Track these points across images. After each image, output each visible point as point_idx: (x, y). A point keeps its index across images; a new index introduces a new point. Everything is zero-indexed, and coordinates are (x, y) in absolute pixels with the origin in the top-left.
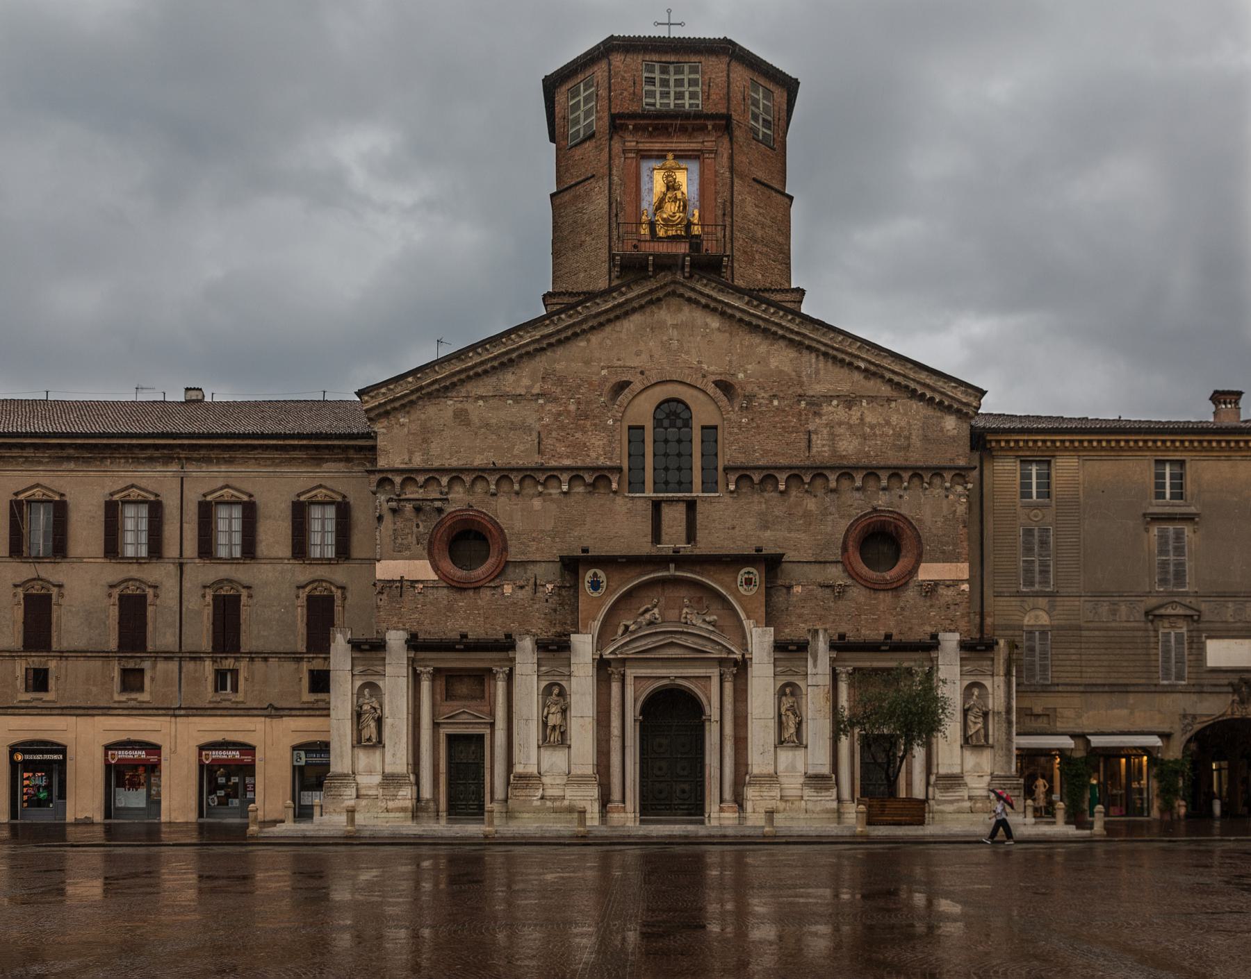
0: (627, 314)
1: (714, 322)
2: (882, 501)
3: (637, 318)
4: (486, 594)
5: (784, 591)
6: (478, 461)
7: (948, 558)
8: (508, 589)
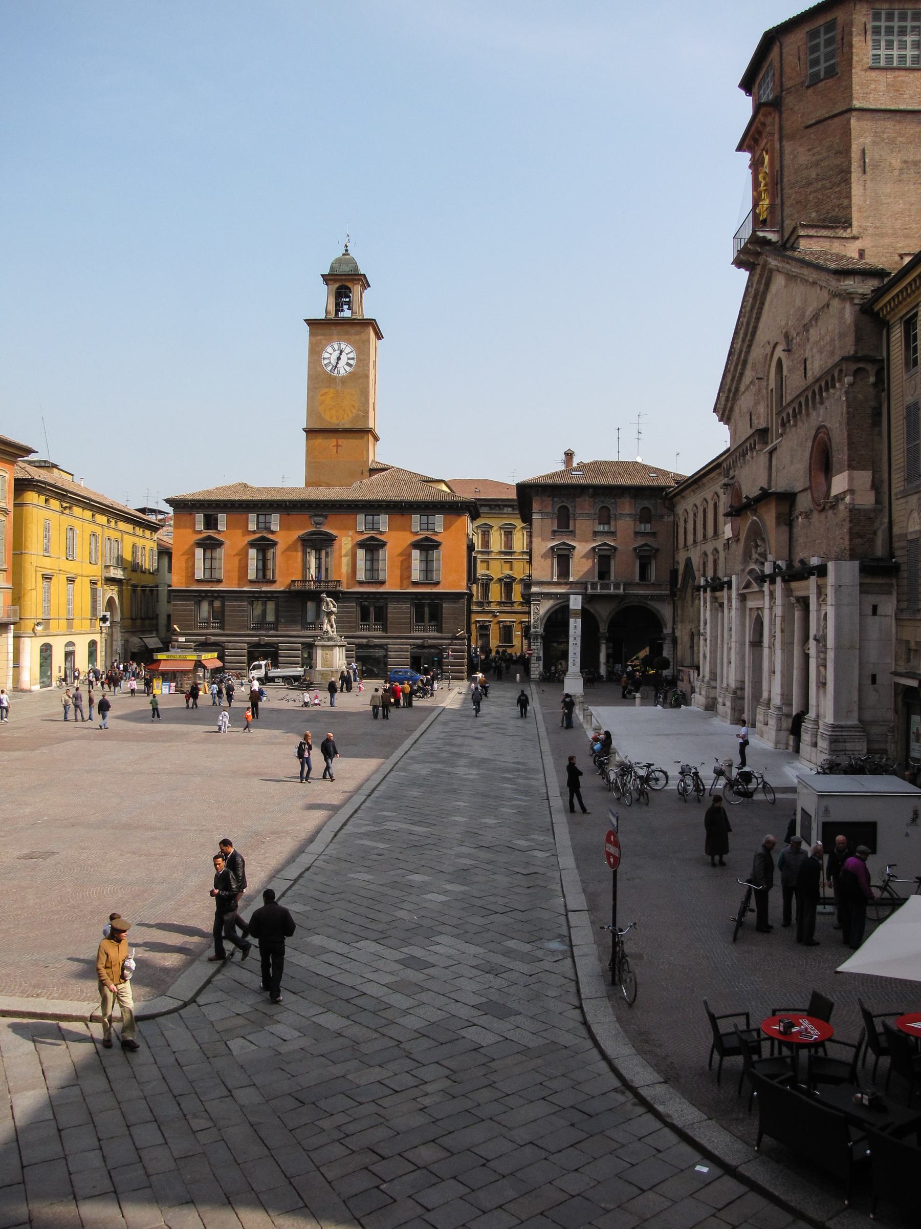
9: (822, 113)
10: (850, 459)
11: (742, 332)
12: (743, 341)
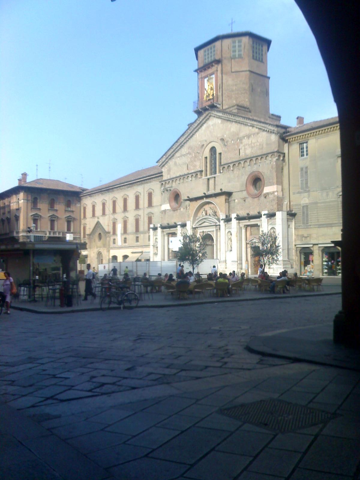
0: (202, 125)
1: (219, 121)
2: (255, 168)
3: (205, 125)
4: (179, 211)
5: (234, 201)
6: (178, 175)
7: (271, 184)
8: (182, 209)
9: (238, 69)
10: (277, 182)
11: (186, 136)
12: (185, 139)
